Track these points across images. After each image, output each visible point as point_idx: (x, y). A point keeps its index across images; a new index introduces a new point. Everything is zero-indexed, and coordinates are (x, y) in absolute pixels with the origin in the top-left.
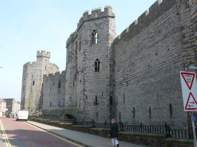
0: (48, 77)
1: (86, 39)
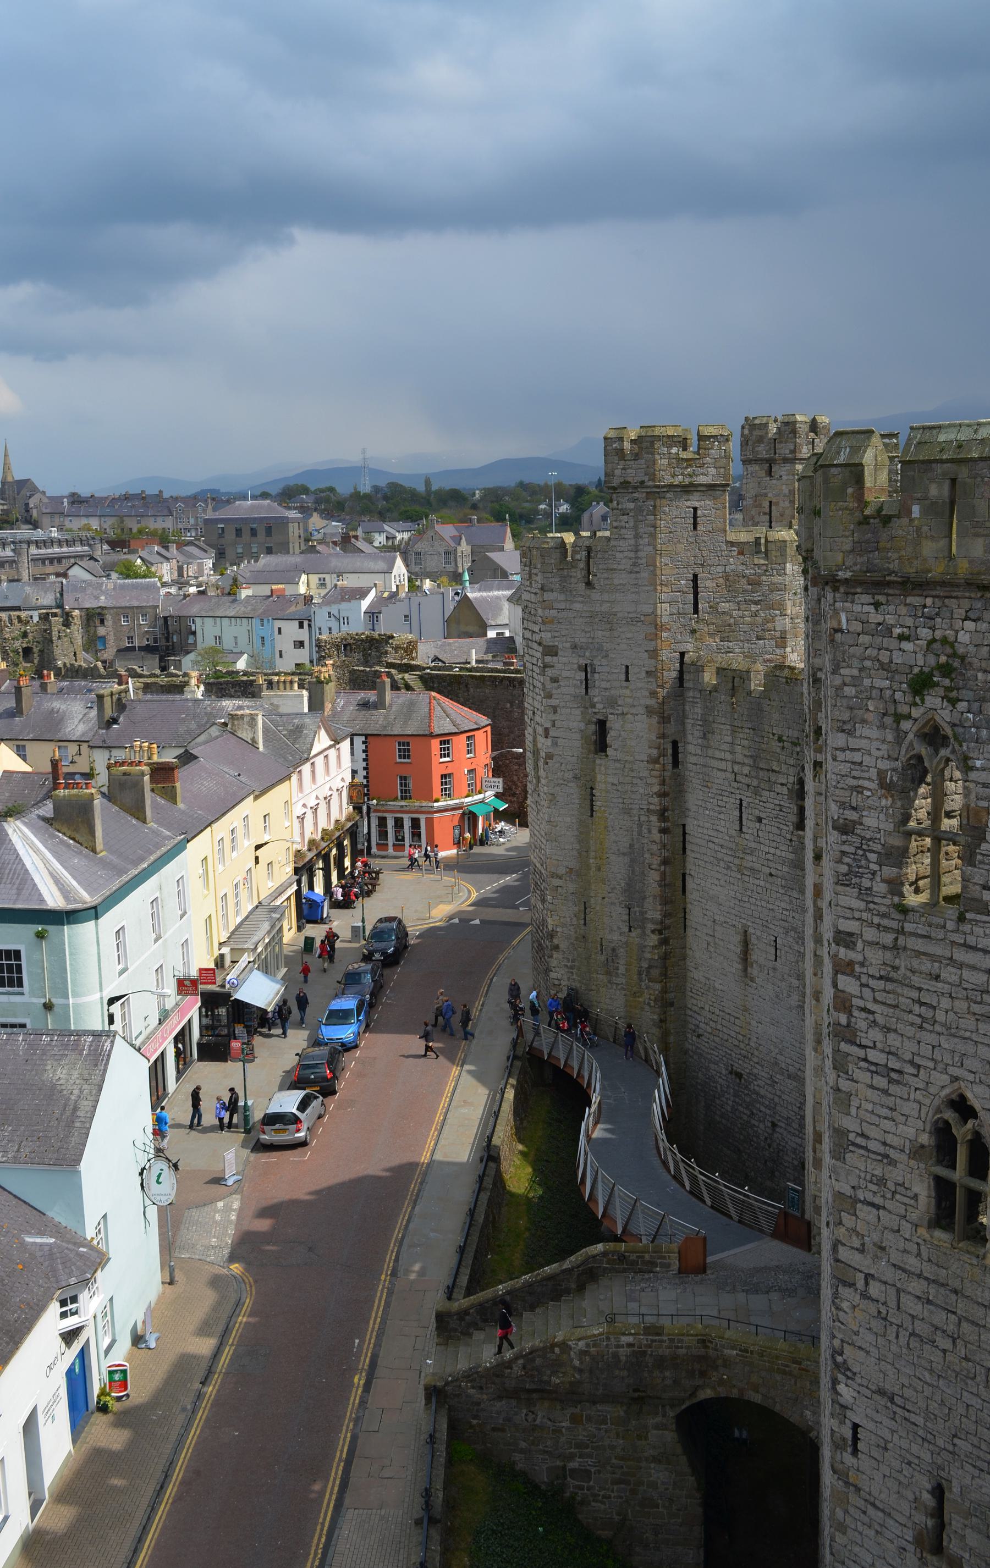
0: (715, 689)
1: (853, 816)
